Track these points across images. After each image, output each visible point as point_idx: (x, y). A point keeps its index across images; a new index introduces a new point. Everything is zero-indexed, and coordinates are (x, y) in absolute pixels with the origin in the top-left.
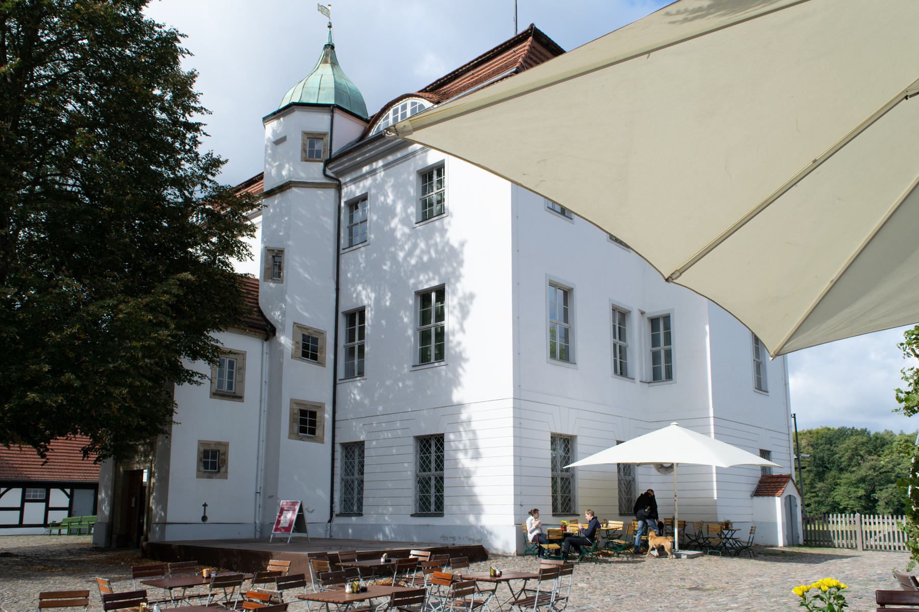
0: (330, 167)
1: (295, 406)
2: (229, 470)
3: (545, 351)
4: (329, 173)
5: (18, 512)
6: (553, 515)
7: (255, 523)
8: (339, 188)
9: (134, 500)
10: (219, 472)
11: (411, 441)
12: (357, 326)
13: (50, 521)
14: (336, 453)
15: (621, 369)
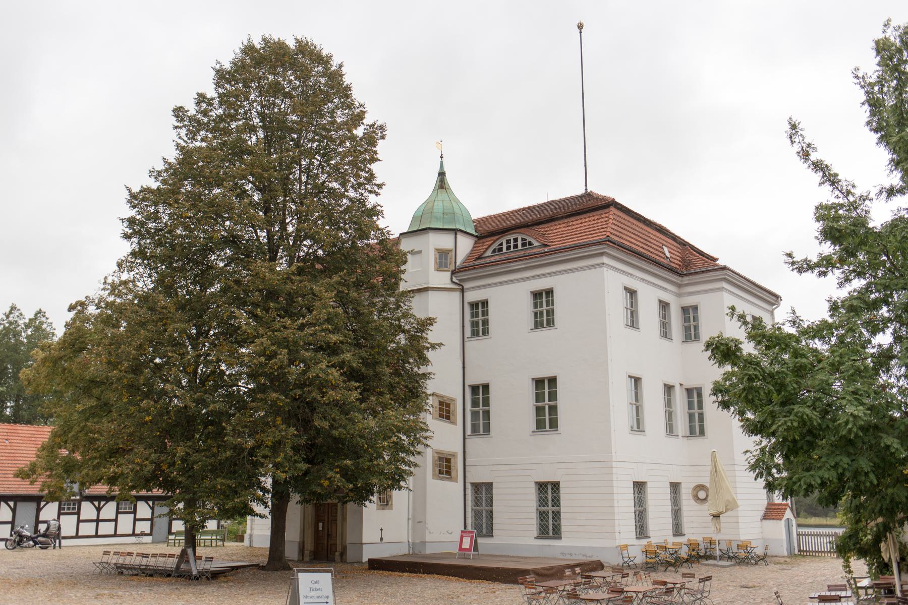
0: (456, 275)
1: (436, 455)
2: (393, 503)
3: (628, 429)
4: (454, 280)
5: (114, 523)
6: (637, 538)
7: (409, 542)
8: (463, 291)
9: (321, 524)
10: (387, 504)
11: (533, 485)
12: (481, 396)
13: (137, 531)
14: (467, 490)
15: (670, 430)
